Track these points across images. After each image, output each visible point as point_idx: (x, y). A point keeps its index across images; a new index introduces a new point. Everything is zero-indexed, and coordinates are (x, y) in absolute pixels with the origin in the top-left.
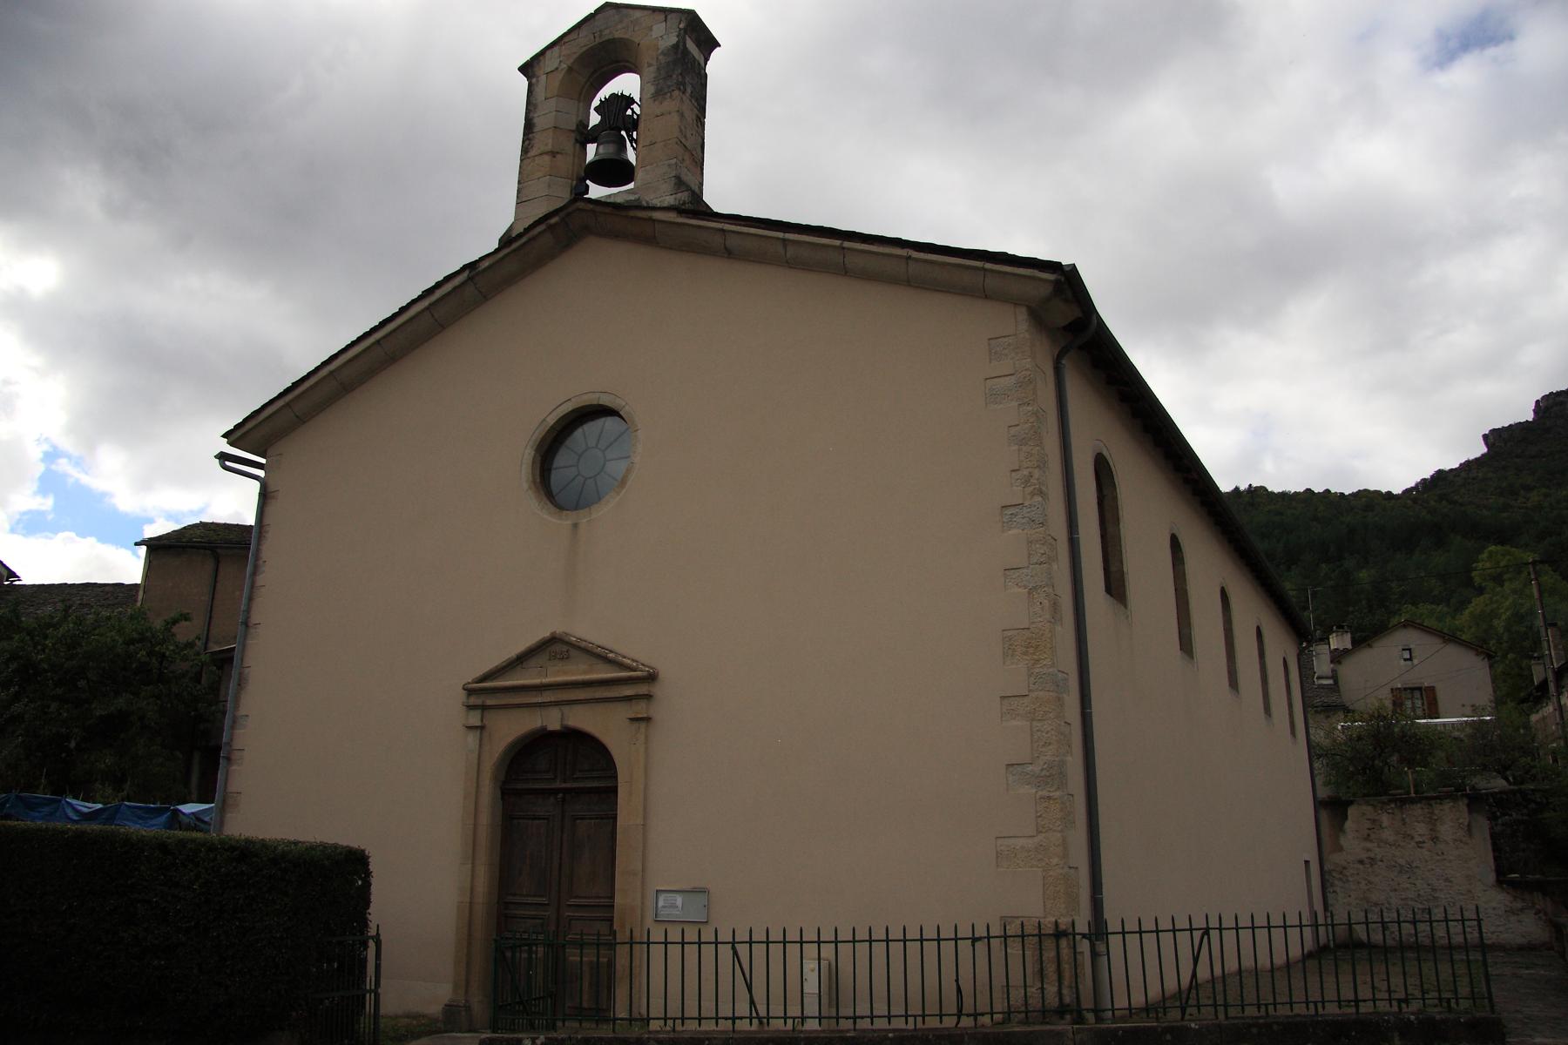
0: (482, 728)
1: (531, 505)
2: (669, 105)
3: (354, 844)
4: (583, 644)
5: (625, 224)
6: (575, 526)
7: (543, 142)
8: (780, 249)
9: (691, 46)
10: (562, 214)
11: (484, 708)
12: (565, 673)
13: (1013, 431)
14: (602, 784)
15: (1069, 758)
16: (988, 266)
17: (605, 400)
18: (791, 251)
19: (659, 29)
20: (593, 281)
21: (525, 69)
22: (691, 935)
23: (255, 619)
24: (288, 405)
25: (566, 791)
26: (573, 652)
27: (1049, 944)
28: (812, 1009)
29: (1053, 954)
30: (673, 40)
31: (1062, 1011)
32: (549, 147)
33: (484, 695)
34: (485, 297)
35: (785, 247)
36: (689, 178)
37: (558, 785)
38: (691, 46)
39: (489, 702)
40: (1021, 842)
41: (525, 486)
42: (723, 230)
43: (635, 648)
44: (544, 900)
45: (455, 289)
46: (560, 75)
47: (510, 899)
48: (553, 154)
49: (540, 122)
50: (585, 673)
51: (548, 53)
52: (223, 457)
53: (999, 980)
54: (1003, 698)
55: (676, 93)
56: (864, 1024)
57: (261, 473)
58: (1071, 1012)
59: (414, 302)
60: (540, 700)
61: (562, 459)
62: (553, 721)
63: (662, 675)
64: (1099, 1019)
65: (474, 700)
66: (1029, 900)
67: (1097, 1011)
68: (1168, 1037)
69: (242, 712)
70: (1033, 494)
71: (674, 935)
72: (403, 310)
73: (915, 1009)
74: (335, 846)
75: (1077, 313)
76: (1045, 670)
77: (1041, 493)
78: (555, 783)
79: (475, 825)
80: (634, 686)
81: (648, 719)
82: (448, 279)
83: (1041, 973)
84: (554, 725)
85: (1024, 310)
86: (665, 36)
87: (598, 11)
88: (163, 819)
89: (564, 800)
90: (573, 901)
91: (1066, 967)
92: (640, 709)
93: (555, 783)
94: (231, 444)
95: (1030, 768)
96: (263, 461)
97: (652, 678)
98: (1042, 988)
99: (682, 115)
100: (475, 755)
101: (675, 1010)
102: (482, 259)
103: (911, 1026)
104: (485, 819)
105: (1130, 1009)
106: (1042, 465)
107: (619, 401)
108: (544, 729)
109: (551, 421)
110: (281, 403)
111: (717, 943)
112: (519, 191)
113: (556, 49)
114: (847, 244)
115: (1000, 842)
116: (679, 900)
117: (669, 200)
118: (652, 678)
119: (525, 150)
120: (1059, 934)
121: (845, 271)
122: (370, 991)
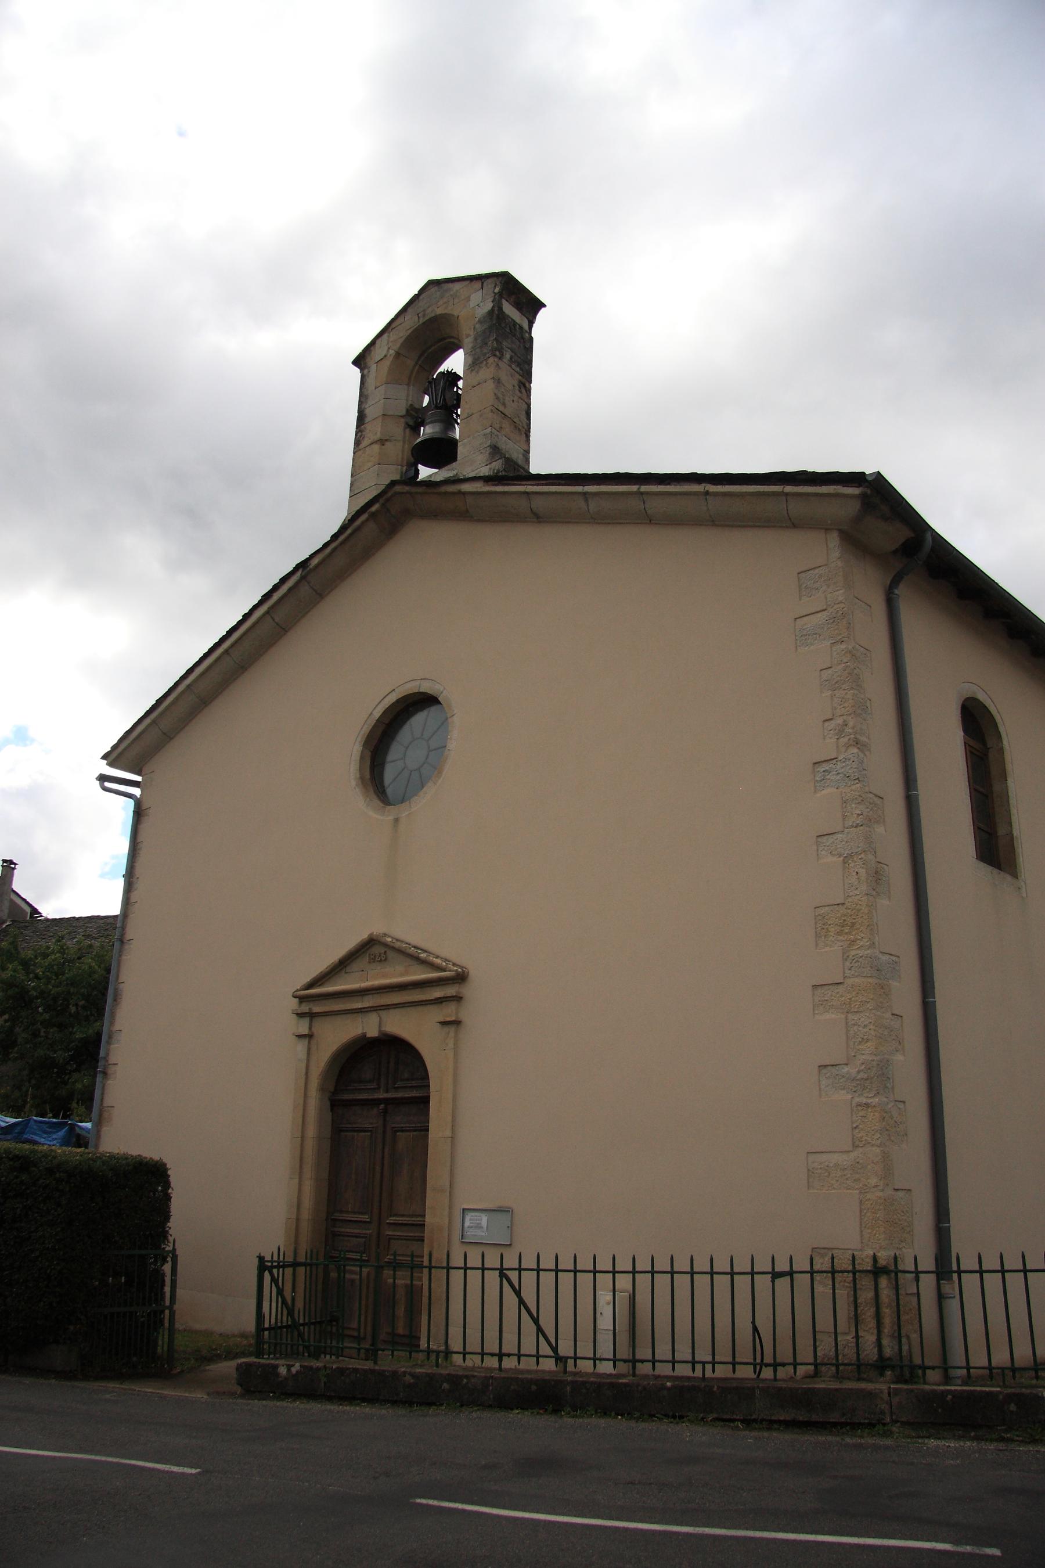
0: (310, 1036)
1: (358, 802)
2: (486, 373)
3: (150, 1152)
4: (398, 945)
5: (448, 505)
6: (397, 820)
7: (374, 431)
8: (582, 504)
9: (509, 309)
10: (382, 501)
11: (312, 1016)
12: (384, 976)
13: (826, 674)
14: (414, 1094)
15: (899, 1057)
16: (789, 489)
17: (426, 687)
18: (593, 505)
19: (476, 297)
20: (423, 563)
21: (359, 361)
22: (492, 1261)
23: (128, 936)
24: (154, 722)
25: (387, 1101)
26: (391, 954)
27: (866, 1283)
28: (605, 1349)
29: (871, 1294)
30: (489, 306)
31: (882, 1365)
32: (378, 436)
33: (315, 1001)
34: (320, 595)
35: (586, 501)
36: (512, 450)
37: (382, 1095)
38: (509, 309)
39: (316, 1009)
40: (835, 1158)
41: (354, 783)
42: (527, 493)
43: (449, 947)
44: (366, 1218)
45: (290, 590)
46: (387, 363)
47: (337, 1215)
48: (382, 442)
49: (370, 413)
50: (402, 975)
51: (378, 342)
52: (103, 778)
53: (824, 1321)
54: (815, 987)
55: (491, 360)
56: (509, 1363)
57: (137, 792)
58: (893, 1368)
59: (255, 608)
60: (360, 1005)
61: (395, 752)
62: (370, 1027)
63: (473, 973)
64: (947, 1379)
65: (305, 1008)
66: (845, 1230)
67: (945, 1368)
68: (1013, 1407)
69: (117, 1027)
70: (848, 746)
71: (474, 1261)
72: (246, 617)
73: (703, 1354)
74: (126, 1157)
75: (905, 533)
76: (861, 953)
77: (857, 742)
78: (374, 1095)
79: (303, 1137)
80: (445, 987)
81: (457, 1023)
82: (284, 580)
83: (857, 1320)
84: (373, 1033)
85: (835, 535)
86: (480, 304)
87: (422, 290)
88: (62, 1133)
89: (385, 1112)
90: (392, 1219)
91: (887, 1313)
92: (448, 1012)
93: (374, 1095)
94: (111, 764)
95: (846, 1069)
96: (139, 779)
97: (461, 978)
98: (857, 1337)
99: (498, 381)
100: (304, 1065)
101: (473, 1345)
102: (312, 556)
103: (698, 1373)
104: (311, 1132)
105: (990, 1368)
106: (861, 709)
107: (437, 687)
108: (364, 1035)
109: (377, 714)
110: (148, 721)
111: (483, 1269)
112: (352, 485)
113: (385, 336)
114: (644, 488)
115: (812, 1157)
116: (484, 1219)
117: (485, 471)
118: (461, 978)
119: (357, 443)
120: (878, 1271)
121: (649, 520)
122: (167, 1307)
